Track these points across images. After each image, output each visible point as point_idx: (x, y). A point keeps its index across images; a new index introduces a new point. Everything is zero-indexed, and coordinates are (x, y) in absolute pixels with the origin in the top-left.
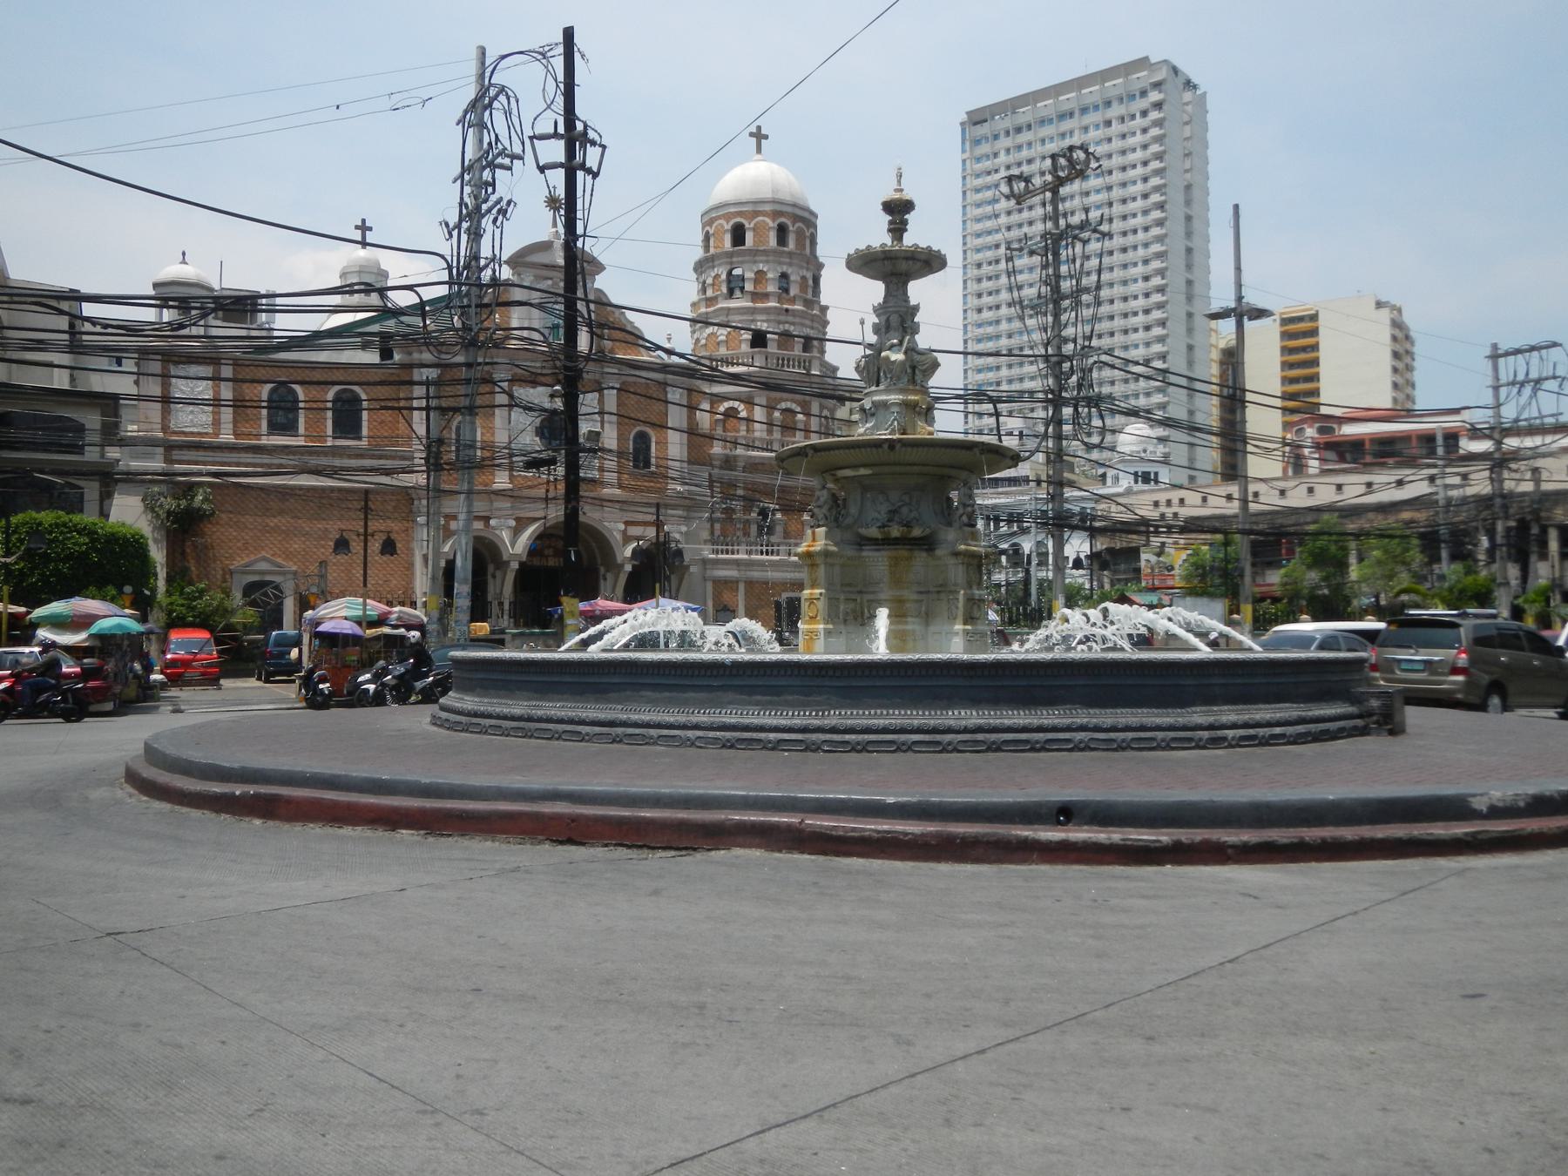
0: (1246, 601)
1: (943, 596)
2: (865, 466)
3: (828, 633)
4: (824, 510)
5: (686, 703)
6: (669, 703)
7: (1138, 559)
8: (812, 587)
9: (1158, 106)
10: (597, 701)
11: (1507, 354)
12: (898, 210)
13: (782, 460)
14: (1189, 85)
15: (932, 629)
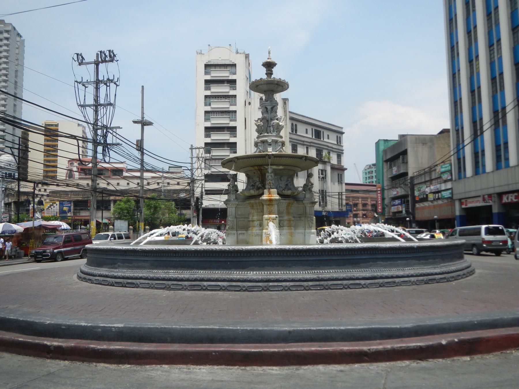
0: (142, 222)
5: (414, 265)
6: (391, 266)
8: (270, 213)
9: (7, 39)
10: (353, 268)
11: (196, 148)
12: (269, 66)
14: (19, 35)
15: (298, 231)
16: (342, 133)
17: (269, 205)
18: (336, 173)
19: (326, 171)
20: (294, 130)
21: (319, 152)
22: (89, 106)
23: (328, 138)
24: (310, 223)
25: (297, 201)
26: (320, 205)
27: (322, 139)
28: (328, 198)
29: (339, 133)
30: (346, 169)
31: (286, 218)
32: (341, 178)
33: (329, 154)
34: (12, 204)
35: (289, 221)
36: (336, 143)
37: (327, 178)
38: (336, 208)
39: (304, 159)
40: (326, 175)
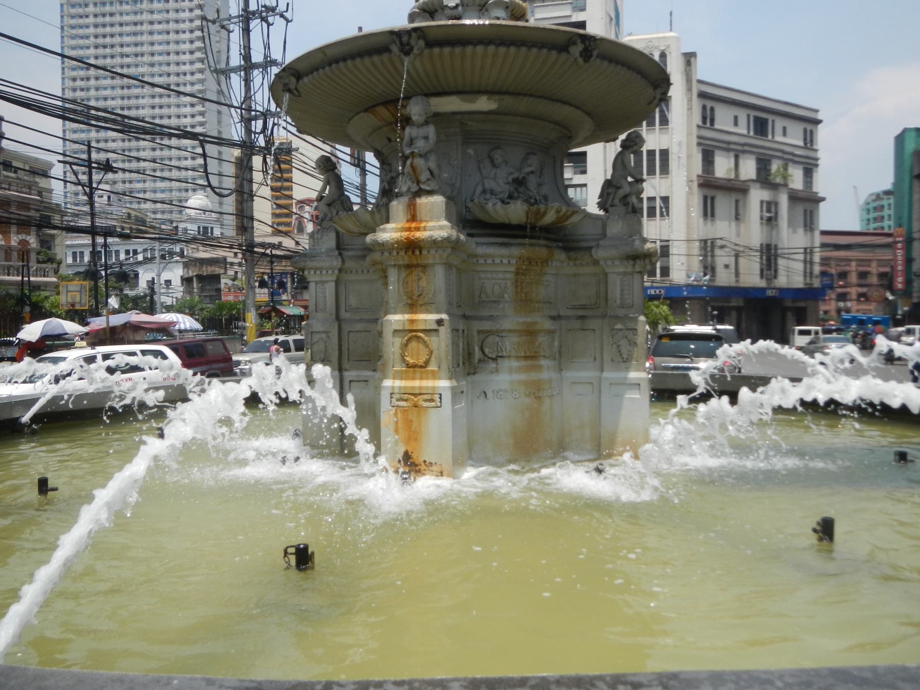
1: (593, 324)
2: (490, 92)
3: (456, 393)
4: (432, 165)
7: (219, 282)
8: (412, 307)
13: (299, 76)
15: (571, 374)
16: (818, 122)
17: (409, 266)
18: (800, 209)
19: (776, 204)
20: (708, 118)
21: (763, 165)
22: (235, 70)
23: (785, 134)
24: (623, 343)
25: (566, 249)
26: (762, 276)
27: (770, 137)
28: (781, 262)
29: (809, 122)
30: (823, 199)
31: (511, 321)
32: (811, 219)
33: (786, 169)
34: (195, 279)
35: (530, 332)
36: (801, 143)
37: (779, 219)
38: (798, 282)
39: (576, 50)
40: (776, 213)
